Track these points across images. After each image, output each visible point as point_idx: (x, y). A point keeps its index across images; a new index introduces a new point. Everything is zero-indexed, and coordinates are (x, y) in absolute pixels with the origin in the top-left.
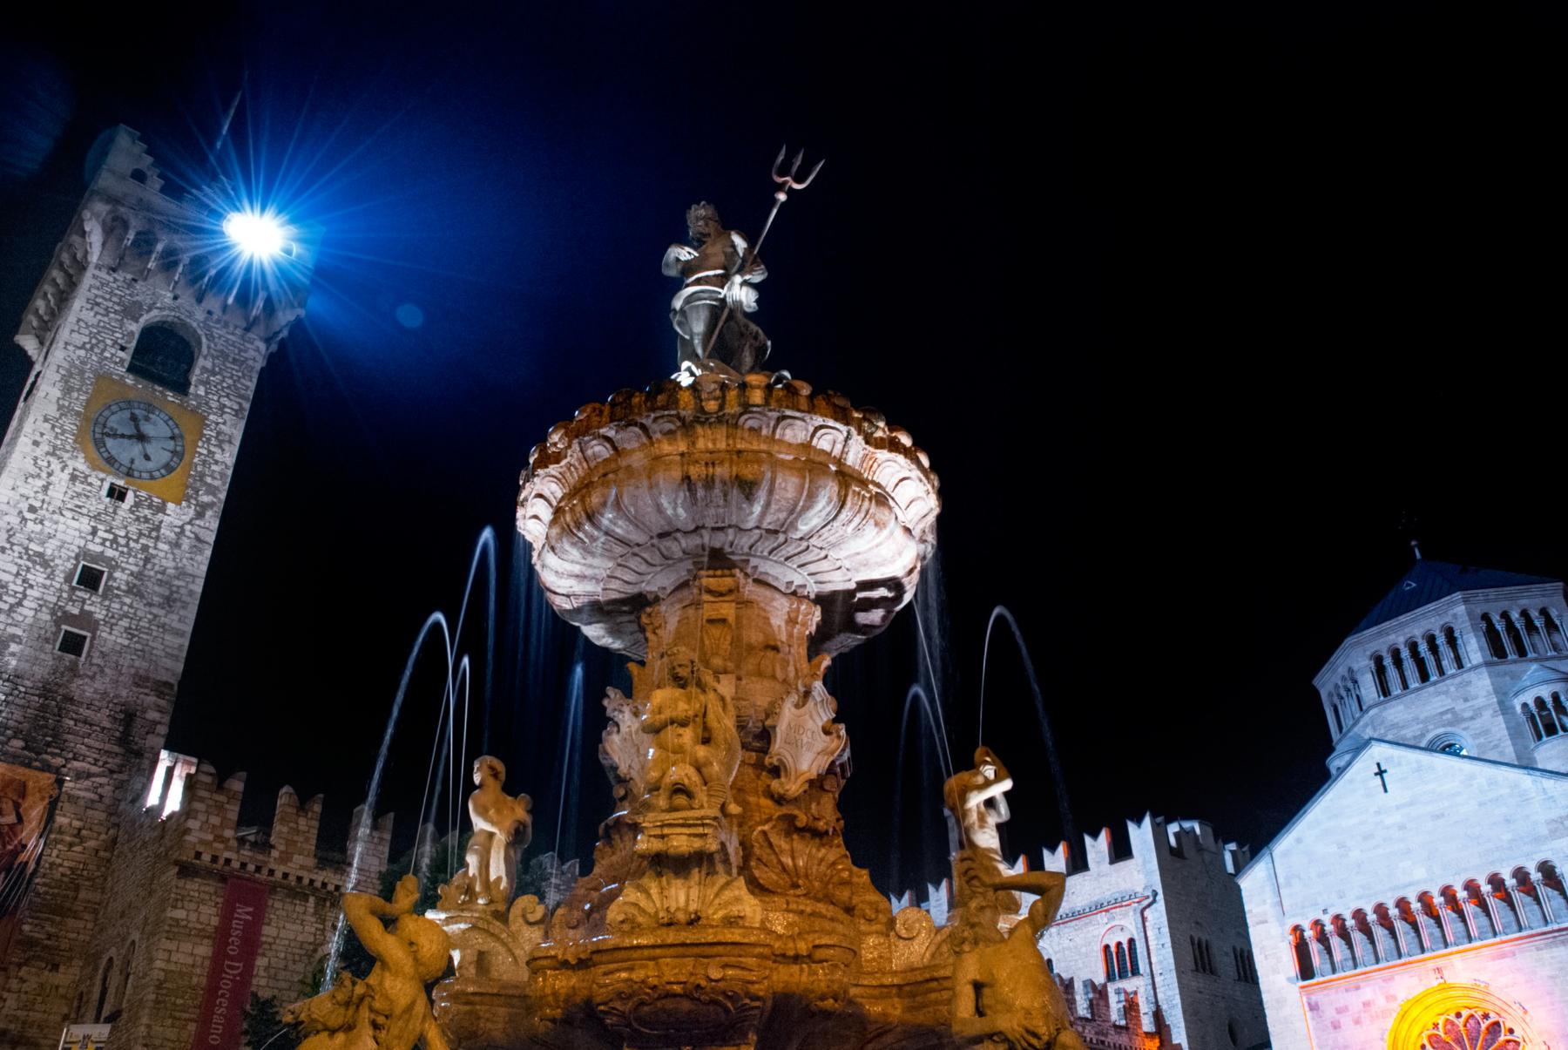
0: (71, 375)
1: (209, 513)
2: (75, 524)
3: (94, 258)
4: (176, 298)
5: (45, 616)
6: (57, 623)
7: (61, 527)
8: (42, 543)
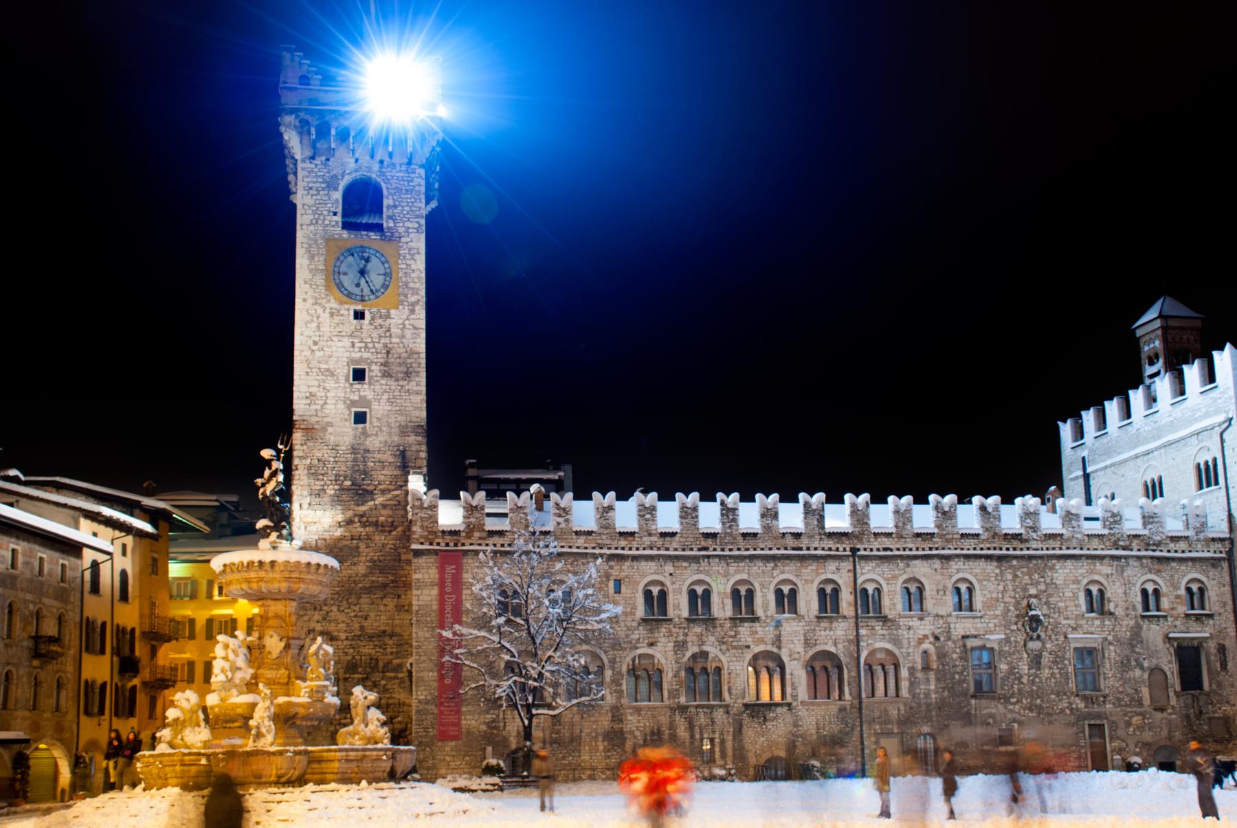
0: (310, 246)
1: (417, 308)
2: (341, 344)
3: (298, 157)
4: (357, 161)
5: (341, 406)
6: (349, 408)
7: (334, 349)
8: (327, 363)
